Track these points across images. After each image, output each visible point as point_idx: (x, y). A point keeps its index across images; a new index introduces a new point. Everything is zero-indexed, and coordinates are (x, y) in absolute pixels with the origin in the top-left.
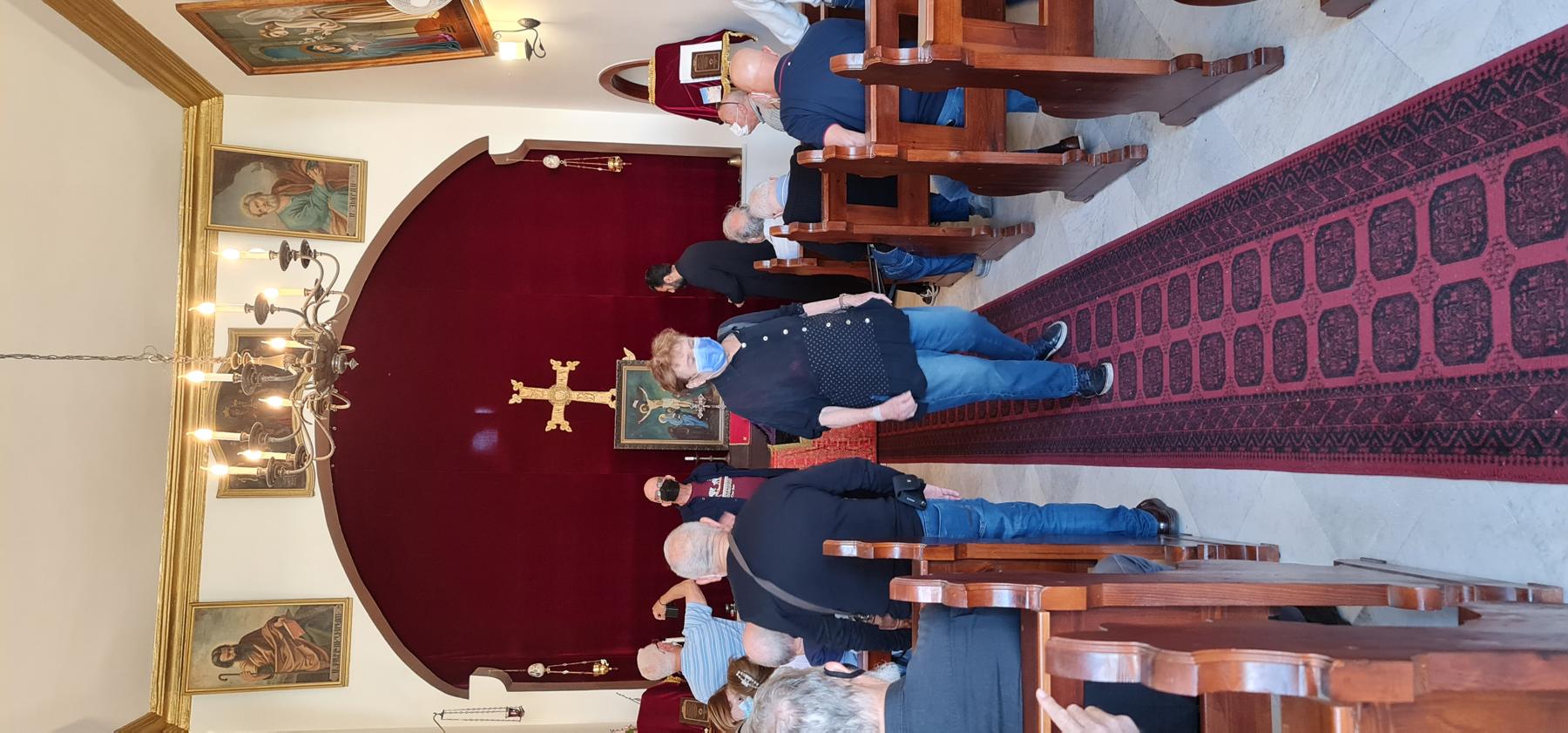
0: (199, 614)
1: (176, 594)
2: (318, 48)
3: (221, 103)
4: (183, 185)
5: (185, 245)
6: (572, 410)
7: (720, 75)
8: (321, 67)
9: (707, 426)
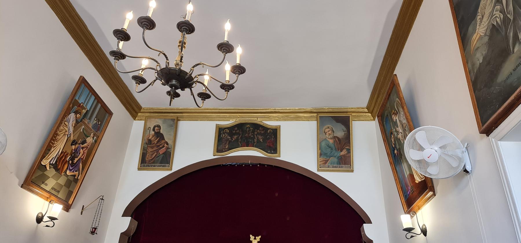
0: (173, 120)
2: (392, 137)
3: (371, 120)
4: (335, 108)
8: (385, 141)
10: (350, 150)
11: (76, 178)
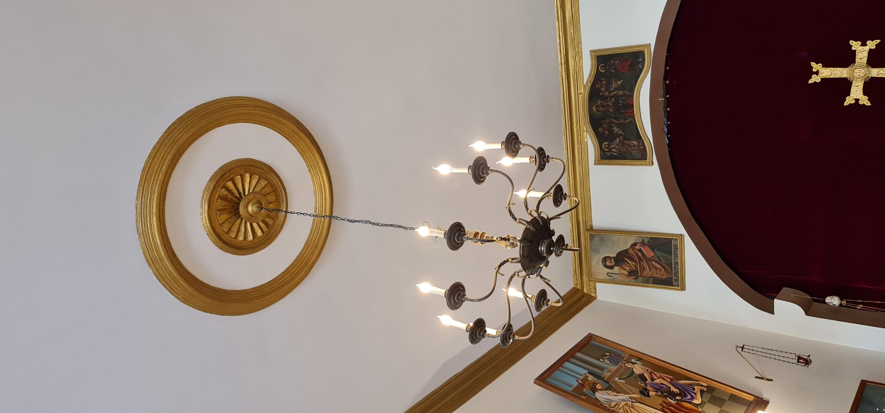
0: (592, 237)
11: (705, 389)
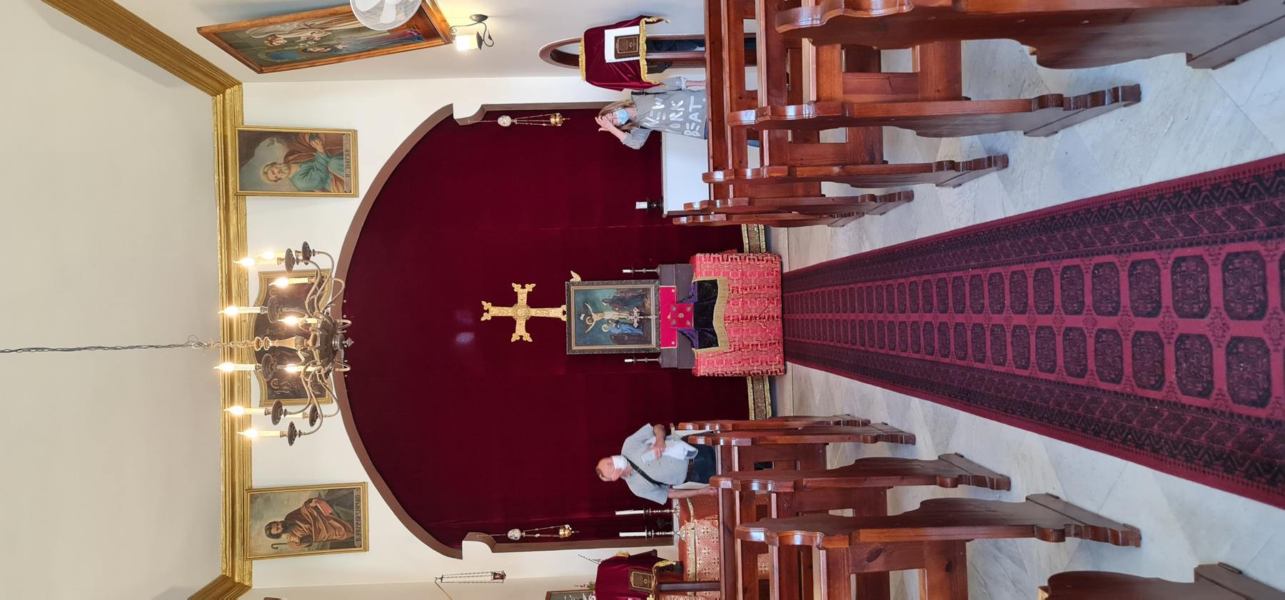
0: (253, 499)
1: (235, 483)
2: (311, 50)
3: (241, 90)
4: (216, 160)
5: (222, 208)
6: (532, 324)
7: (639, 56)
8: (315, 63)
9: (641, 333)
10: (311, 133)
